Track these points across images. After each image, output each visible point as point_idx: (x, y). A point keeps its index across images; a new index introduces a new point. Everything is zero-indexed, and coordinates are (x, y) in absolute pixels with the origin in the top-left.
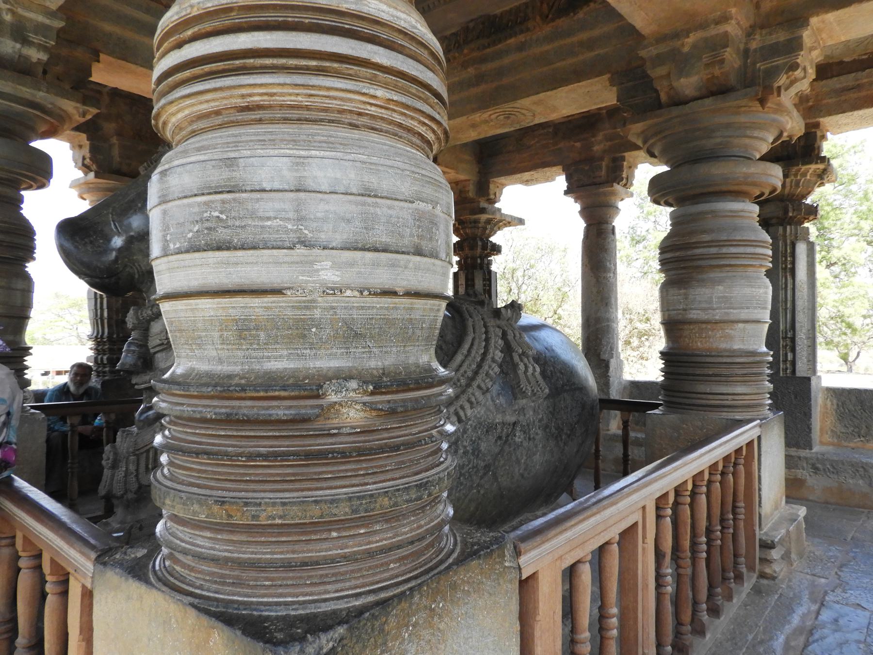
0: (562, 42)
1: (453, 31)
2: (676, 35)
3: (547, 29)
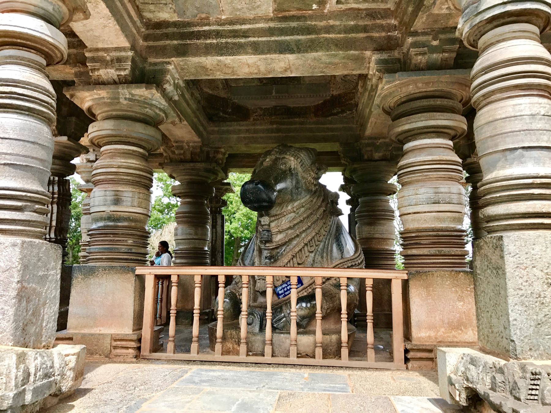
0: (320, 126)
1: (268, 107)
2: (376, 138)
3: (315, 119)
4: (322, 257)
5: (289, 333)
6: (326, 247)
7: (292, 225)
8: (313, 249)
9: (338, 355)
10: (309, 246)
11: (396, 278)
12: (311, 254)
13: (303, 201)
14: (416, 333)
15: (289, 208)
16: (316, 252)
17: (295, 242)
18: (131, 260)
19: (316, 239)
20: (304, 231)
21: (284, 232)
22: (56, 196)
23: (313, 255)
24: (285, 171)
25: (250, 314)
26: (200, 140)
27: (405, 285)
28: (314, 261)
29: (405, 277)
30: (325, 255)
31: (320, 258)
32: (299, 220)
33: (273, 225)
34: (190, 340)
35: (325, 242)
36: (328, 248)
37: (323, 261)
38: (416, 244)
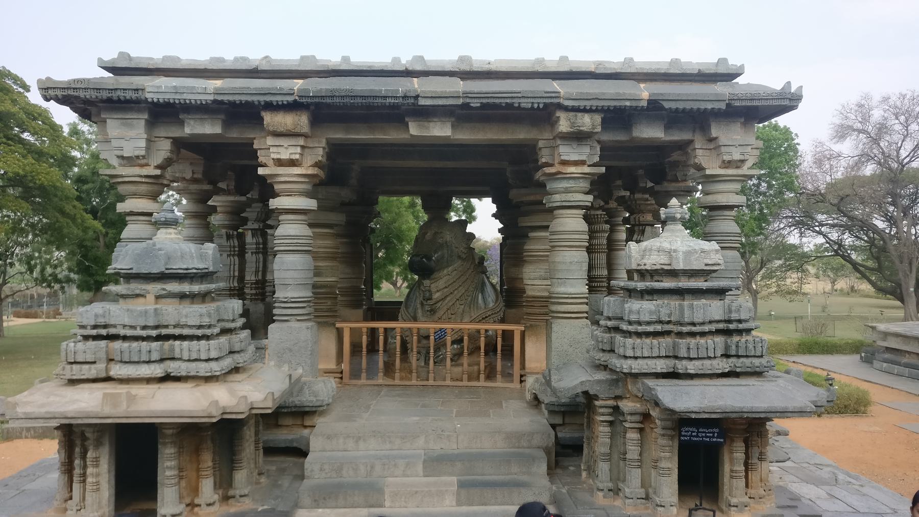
4: (470, 308)
5: (445, 366)
8: (462, 302)
9: (478, 379)
11: (517, 329)
13: (455, 265)
14: (527, 365)
17: (448, 298)
18: (330, 316)
19: (465, 294)
22: (237, 249)
25: (419, 353)
27: (523, 335)
28: (463, 311)
29: (523, 328)
30: (472, 306)
31: (468, 308)
33: (433, 286)
34: (360, 370)
38: (532, 306)
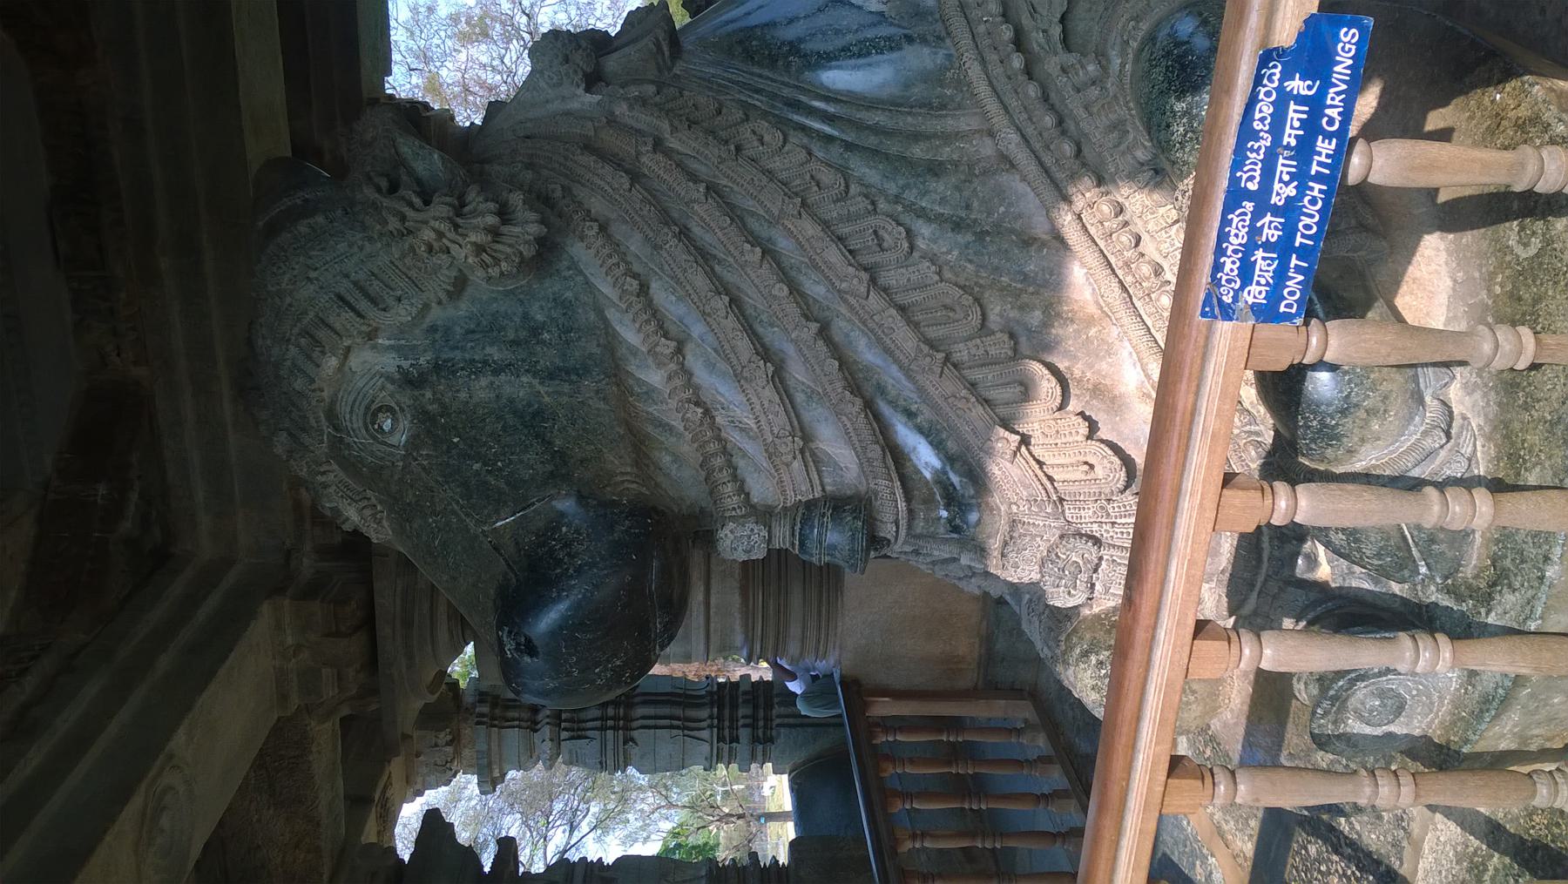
4: (935, 169)
6: (872, 141)
7: (763, 370)
10: (878, 258)
12: (921, 243)
15: (655, 377)
16: (910, 208)
17: (866, 353)
20: (795, 290)
21: (807, 416)
23: (924, 230)
24: (424, 418)
26: (266, 608)
28: (958, 226)
30: (918, 151)
31: (939, 187)
32: (731, 323)
35: (849, 146)
36: (876, 130)
37: (956, 164)
